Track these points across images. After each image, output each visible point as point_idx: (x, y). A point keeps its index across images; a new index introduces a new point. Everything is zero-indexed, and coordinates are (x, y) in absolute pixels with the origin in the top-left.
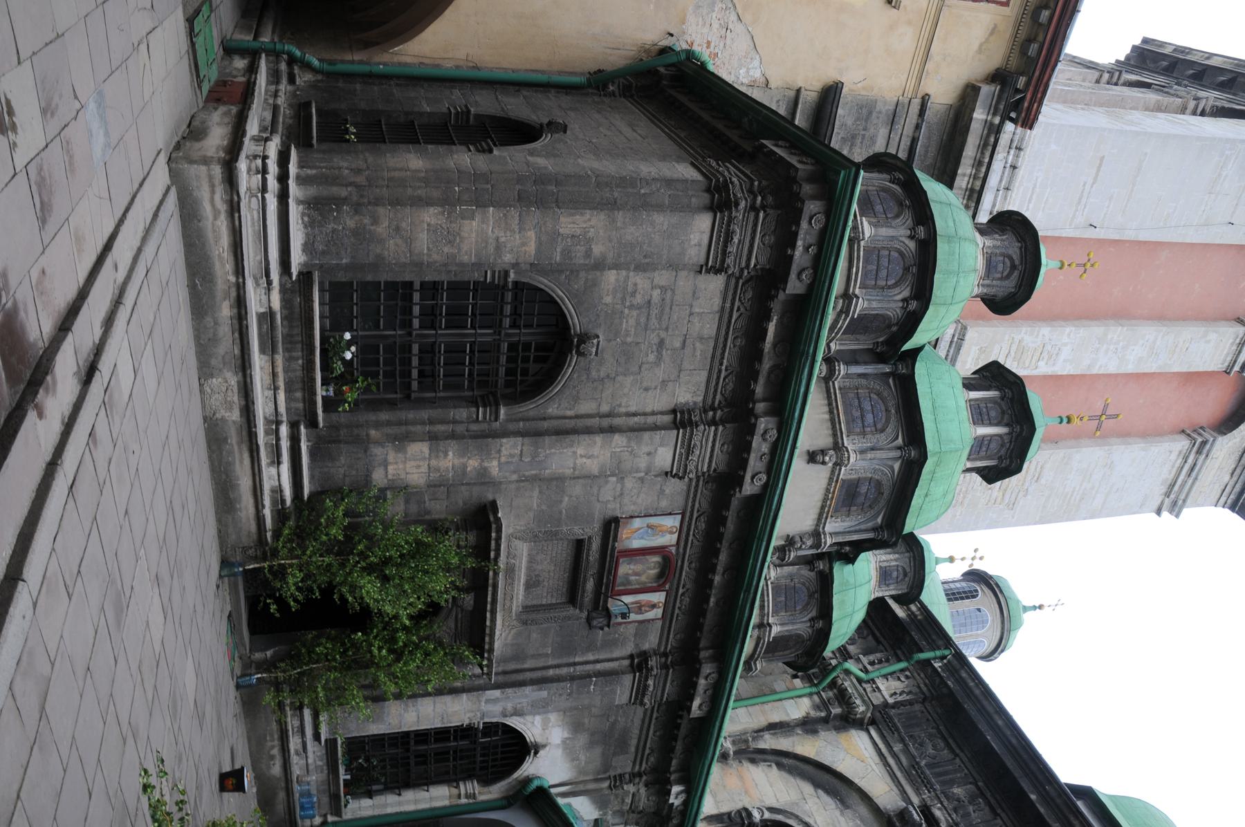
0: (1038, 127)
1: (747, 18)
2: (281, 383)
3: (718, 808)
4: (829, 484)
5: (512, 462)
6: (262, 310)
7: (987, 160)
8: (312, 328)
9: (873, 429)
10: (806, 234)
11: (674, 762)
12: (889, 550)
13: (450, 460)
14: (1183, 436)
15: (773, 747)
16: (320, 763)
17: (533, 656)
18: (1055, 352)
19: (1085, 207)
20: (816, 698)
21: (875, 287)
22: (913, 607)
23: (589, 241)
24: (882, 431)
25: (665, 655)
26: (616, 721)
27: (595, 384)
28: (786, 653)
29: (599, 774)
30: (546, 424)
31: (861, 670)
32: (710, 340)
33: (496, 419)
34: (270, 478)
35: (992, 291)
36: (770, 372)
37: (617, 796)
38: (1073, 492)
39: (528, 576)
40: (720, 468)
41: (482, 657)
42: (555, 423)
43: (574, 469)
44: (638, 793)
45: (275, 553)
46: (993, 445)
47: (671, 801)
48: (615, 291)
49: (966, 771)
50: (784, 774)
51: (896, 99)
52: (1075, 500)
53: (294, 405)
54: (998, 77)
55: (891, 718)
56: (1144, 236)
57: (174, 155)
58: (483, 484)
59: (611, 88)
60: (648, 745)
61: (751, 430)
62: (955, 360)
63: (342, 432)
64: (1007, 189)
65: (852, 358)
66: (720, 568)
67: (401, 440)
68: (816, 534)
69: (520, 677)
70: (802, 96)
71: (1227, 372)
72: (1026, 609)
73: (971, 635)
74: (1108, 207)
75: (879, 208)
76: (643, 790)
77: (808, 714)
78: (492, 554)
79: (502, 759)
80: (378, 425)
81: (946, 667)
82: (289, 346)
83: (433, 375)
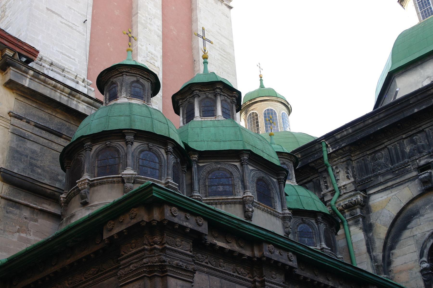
7: (54, 82)
9: (230, 179)
15: (381, 251)
18: (150, 55)
19: (73, 24)
20: (350, 222)
24: (231, 174)
38: (220, 55)
40: (283, 279)
49: (396, 143)
51: (10, 133)
52: (225, 54)
61: (269, 259)
64: (63, 70)
66: (326, 282)
68: (284, 218)
72: (262, 86)
74: (74, 10)
75: (111, 161)
77: (361, 228)
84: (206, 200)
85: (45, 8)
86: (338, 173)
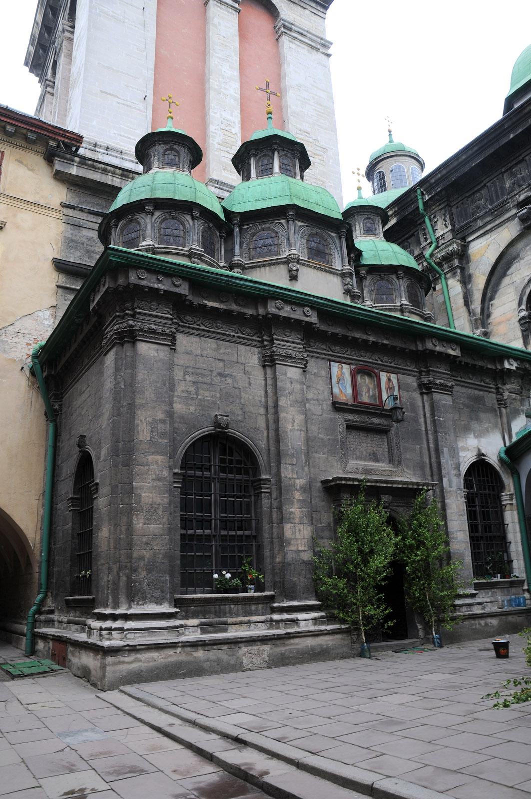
0: (82, 133)
1: (11, 320)
2: (246, 619)
3: (519, 338)
4: (311, 267)
5: (297, 471)
6: (199, 631)
7: (103, 166)
8: (211, 599)
9: (275, 238)
10: (150, 281)
11: (489, 366)
12: (353, 229)
13: (295, 510)
14: (280, 40)
16: (490, 593)
17: (421, 457)
20: (448, 276)
21: (184, 237)
22: (390, 213)
23: (154, 421)
24: (277, 233)
25: (420, 372)
26: (463, 404)
27: (246, 417)
28: (419, 295)
29: (497, 415)
30: (272, 449)
31: (430, 246)
32: (218, 343)
33: (269, 480)
34: (307, 626)
35: (187, 162)
36: (239, 305)
37: (511, 403)
38: (316, 110)
39: (370, 460)
41: (422, 489)
42: (272, 443)
43: (301, 430)
44: (509, 389)
45: (355, 623)
46: (286, 162)
47: (515, 369)
48: (187, 404)
50: (497, 295)
53: (260, 611)
54: (49, 159)
55: (461, 228)
56: (152, 65)
57: (100, 688)
58: (310, 489)
59: (57, 407)
60: (479, 383)
61: (276, 317)
62: (231, 186)
63: (278, 580)
65: (230, 252)
66: (365, 337)
67: (283, 541)
68: (343, 275)
69: (435, 465)
70: (62, 285)
71: (239, 12)
72: (391, 141)
75: (133, 235)
76: (508, 387)
78: (356, 483)
79: (487, 477)
80: (273, 557)
81: (428, 193)
82: (222, 613)
83: (241, 521)
84: (249, 264)
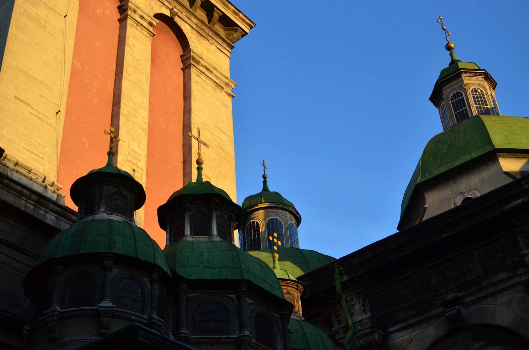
7: (19, 188)
18: (133, 153)
19: (45, 116)
31: (346, 332)
38: (217, 153)
56: (67, 78)
72: (265, 188)
73: (285, 233)
74: (46, 99)
85: (13, 96)
86: (353, 305)
